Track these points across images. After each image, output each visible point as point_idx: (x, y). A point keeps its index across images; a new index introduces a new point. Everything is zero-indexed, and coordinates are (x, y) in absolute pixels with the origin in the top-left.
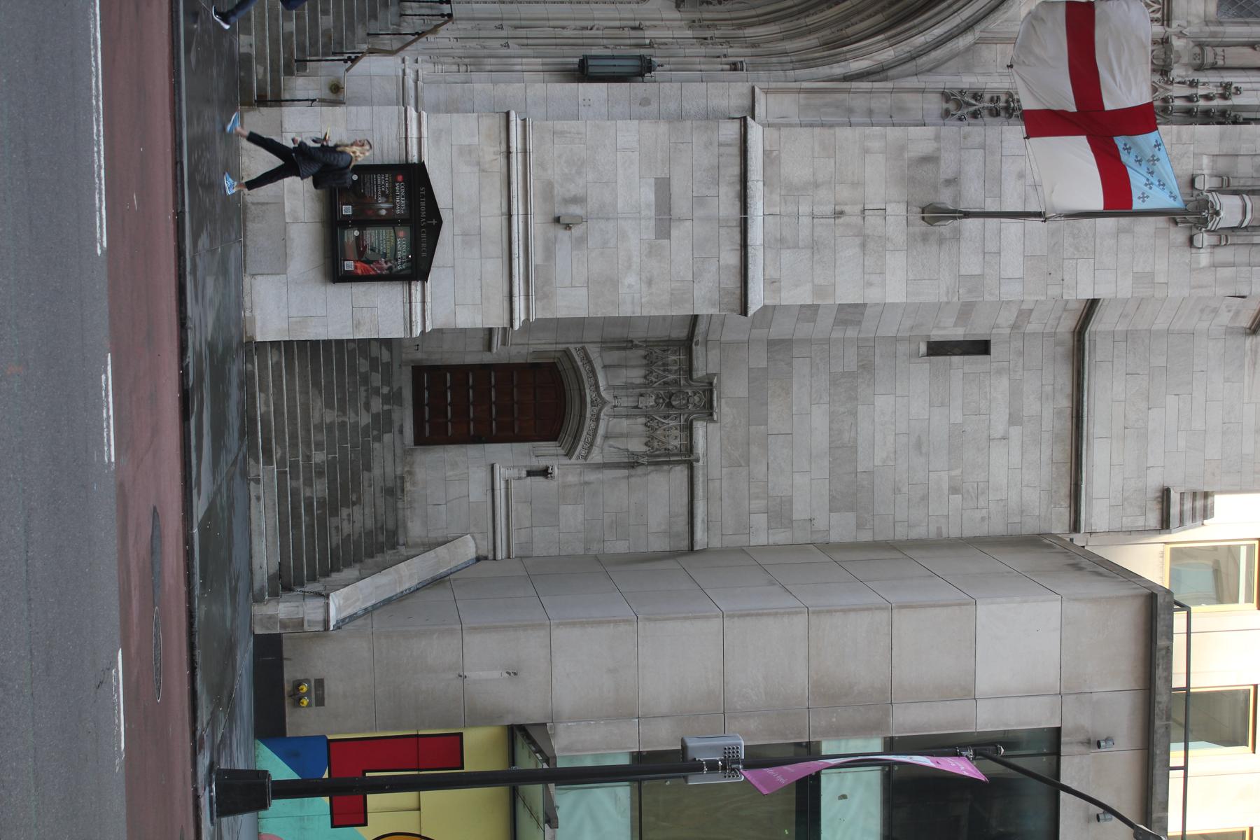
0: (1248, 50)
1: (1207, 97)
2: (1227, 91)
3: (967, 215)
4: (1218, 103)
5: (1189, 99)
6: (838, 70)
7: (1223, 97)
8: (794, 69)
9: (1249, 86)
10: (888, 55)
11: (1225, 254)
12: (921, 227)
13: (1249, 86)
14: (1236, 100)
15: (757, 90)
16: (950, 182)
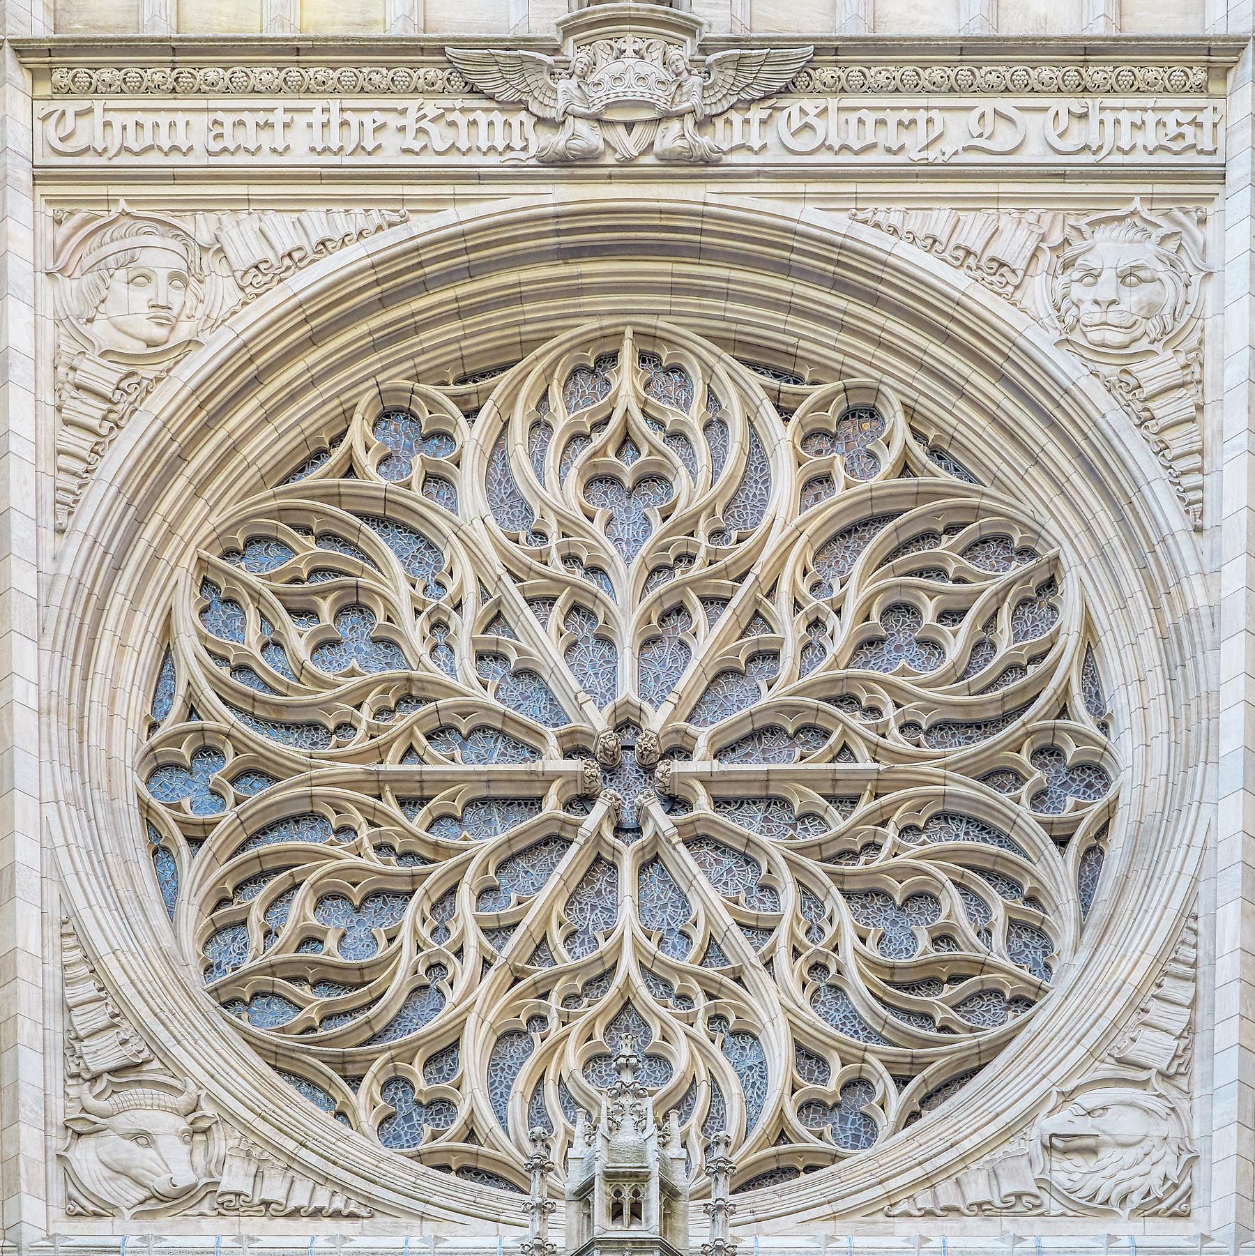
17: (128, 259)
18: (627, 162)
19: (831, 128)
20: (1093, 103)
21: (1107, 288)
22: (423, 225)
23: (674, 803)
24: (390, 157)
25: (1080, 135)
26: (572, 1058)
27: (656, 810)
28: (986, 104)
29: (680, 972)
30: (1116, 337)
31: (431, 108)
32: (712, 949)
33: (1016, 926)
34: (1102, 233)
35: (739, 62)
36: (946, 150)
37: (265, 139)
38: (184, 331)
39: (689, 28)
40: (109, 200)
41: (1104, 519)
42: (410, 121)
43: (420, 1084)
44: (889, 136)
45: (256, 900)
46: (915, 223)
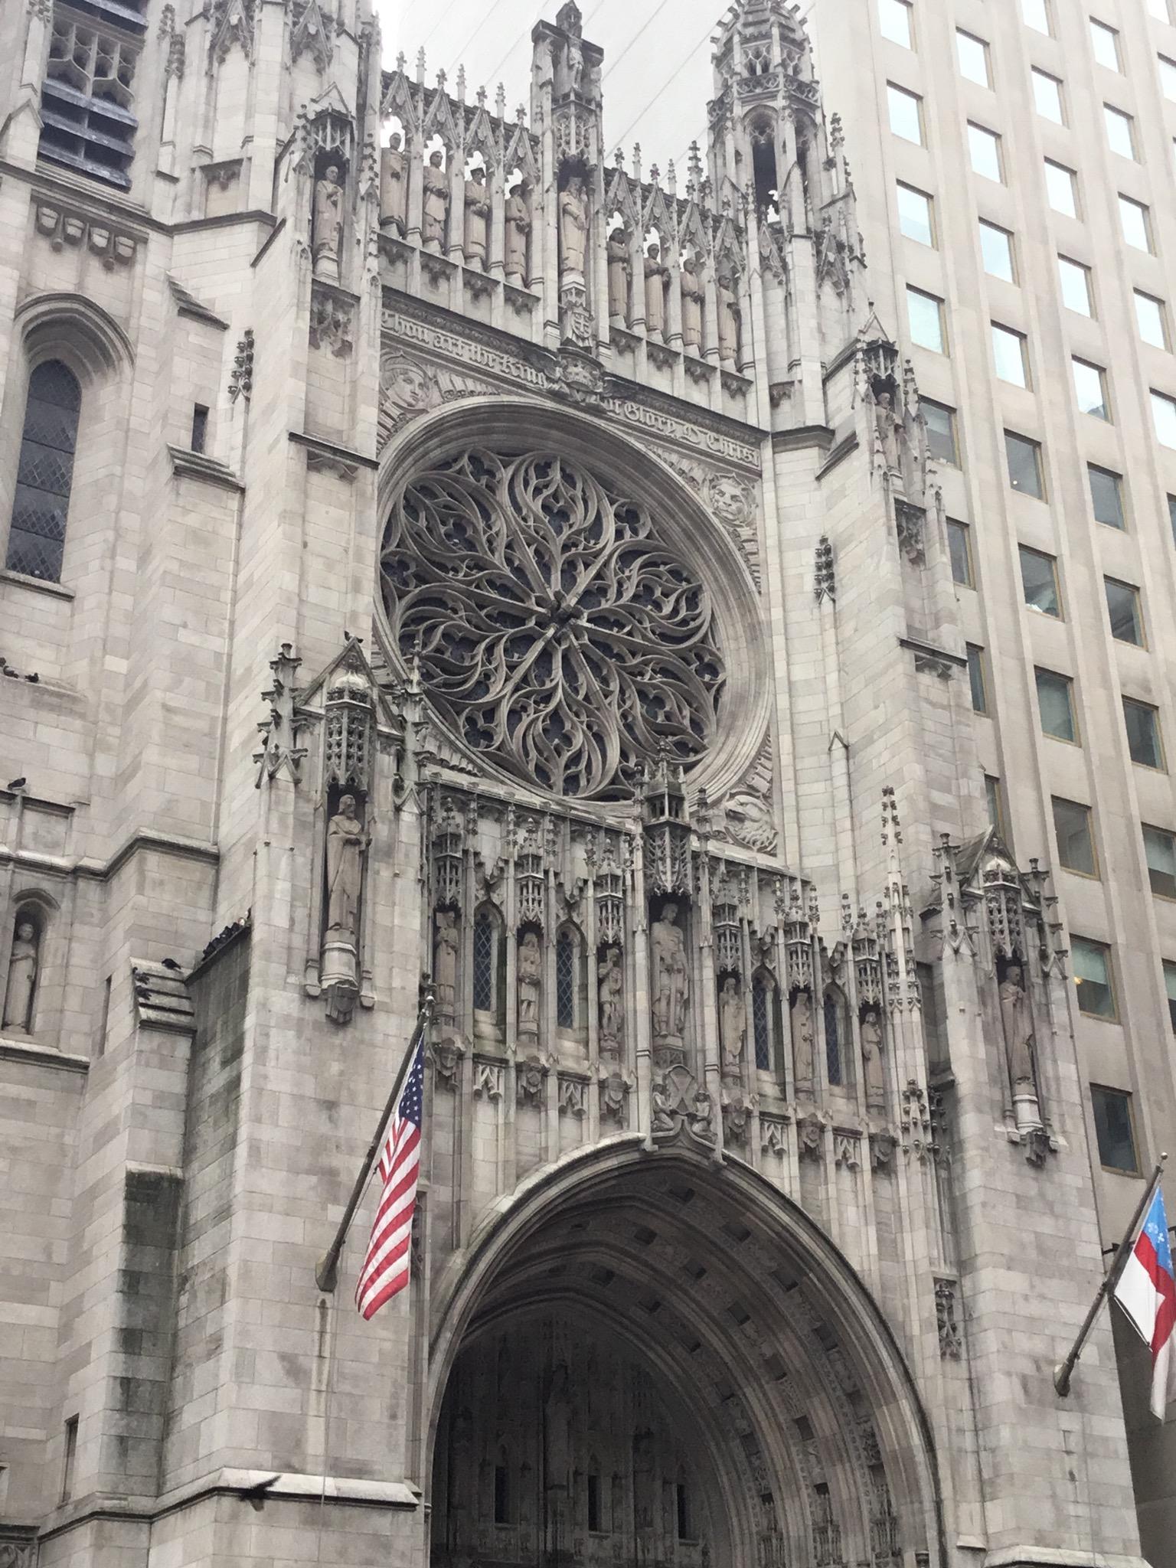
0: (871, 1065)
1: (922, 1112)
2: (913, 1093)
3: (1075, 1355)
4: (925, 1101)
5: (925, 1128)
6: (920, 1457)
7: (920, 1097)
8: (921, 1503)
9: (901, 1071)
10: (906, 1406)
11: (1056, 1125)
12: (1070, 1399)
13: (901, 1071)
14: (922, 1084)
15: (960, 1544)
16: (1038, 1368)
17: (405, 372)
18: (577, 402)
19: (640, 415)
20: (721, 437)
21: (727, 499)
22: (506, 399)
23: (577, 639)
24: (496, 370)
25: (715, 446)
26: (540, 726)
27: (572, 637)
28: (688, 425)
29: (578, 702)
30: (730, 517)
31: (512, 360)
32: (587, 698)
33: (692, 721)
34: (724, 480)
35: (615, 384)
36: (678, 435)
37: (455, 350)
38: (420, 405)
39: (599, 365)
40: (398, 349)
41: (724, 579)
42: (504, 361)
43: (481, 723)
44: (661, 426)
45: (422, 627)
46: (666, 455)
